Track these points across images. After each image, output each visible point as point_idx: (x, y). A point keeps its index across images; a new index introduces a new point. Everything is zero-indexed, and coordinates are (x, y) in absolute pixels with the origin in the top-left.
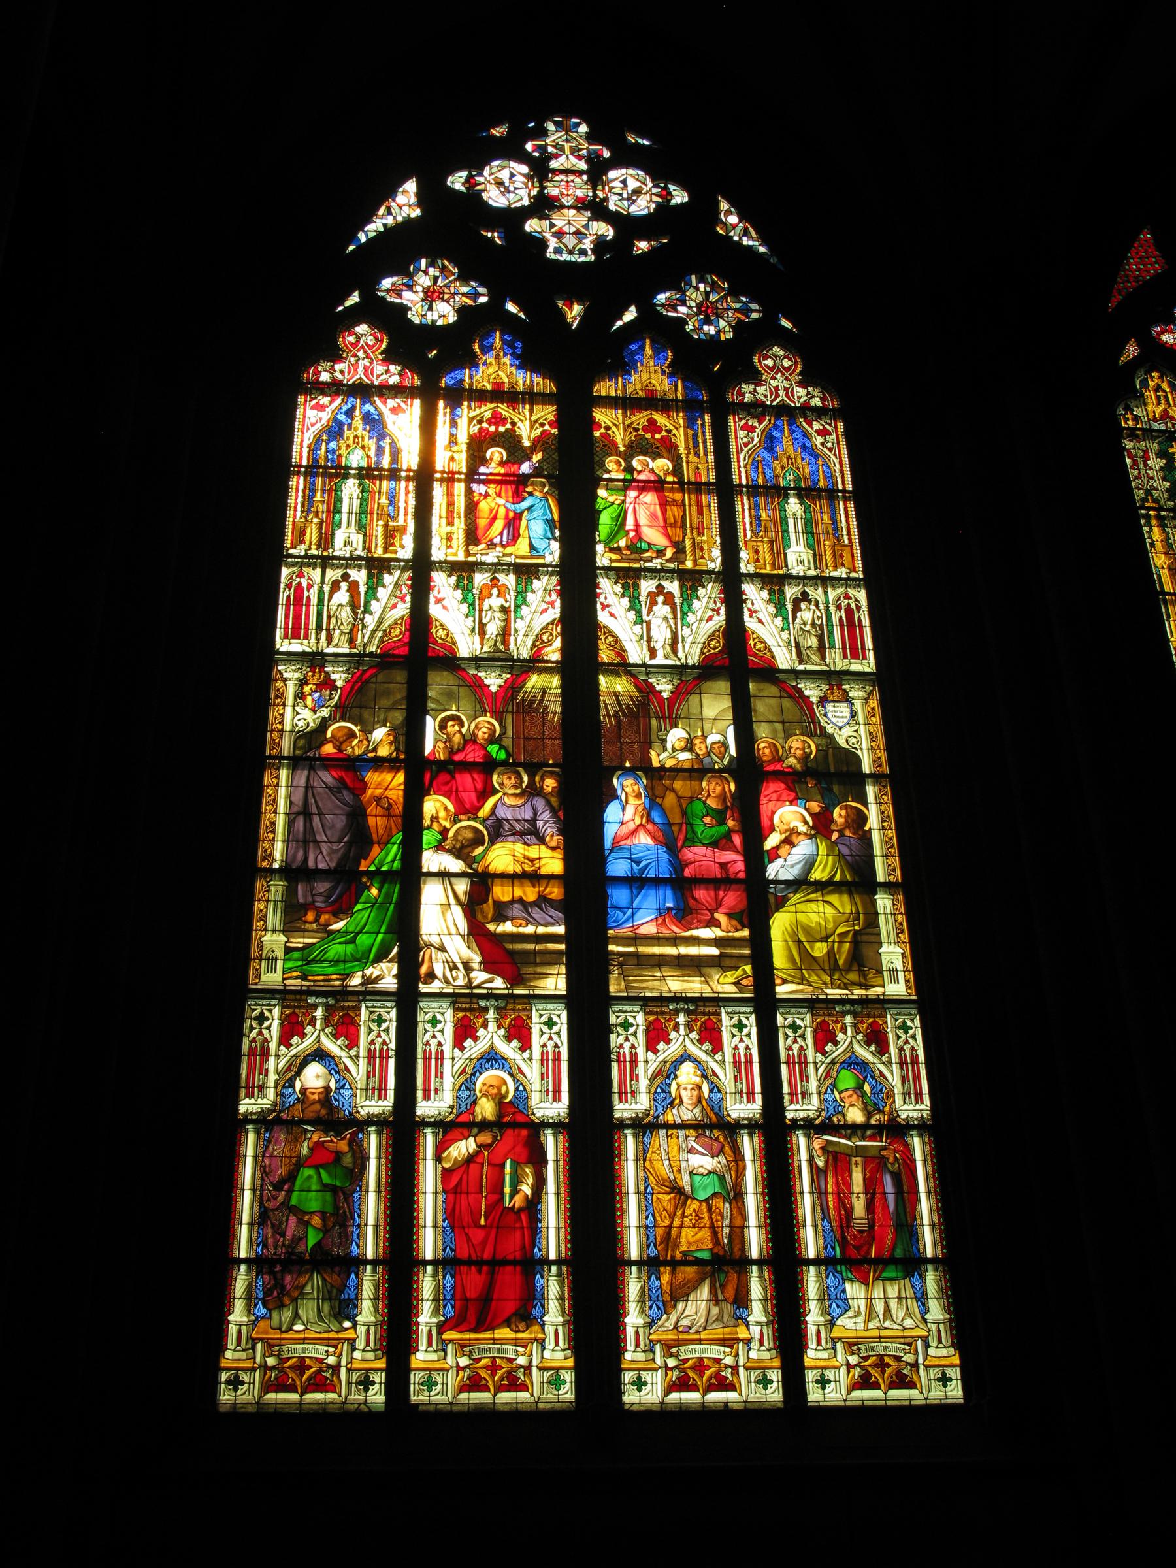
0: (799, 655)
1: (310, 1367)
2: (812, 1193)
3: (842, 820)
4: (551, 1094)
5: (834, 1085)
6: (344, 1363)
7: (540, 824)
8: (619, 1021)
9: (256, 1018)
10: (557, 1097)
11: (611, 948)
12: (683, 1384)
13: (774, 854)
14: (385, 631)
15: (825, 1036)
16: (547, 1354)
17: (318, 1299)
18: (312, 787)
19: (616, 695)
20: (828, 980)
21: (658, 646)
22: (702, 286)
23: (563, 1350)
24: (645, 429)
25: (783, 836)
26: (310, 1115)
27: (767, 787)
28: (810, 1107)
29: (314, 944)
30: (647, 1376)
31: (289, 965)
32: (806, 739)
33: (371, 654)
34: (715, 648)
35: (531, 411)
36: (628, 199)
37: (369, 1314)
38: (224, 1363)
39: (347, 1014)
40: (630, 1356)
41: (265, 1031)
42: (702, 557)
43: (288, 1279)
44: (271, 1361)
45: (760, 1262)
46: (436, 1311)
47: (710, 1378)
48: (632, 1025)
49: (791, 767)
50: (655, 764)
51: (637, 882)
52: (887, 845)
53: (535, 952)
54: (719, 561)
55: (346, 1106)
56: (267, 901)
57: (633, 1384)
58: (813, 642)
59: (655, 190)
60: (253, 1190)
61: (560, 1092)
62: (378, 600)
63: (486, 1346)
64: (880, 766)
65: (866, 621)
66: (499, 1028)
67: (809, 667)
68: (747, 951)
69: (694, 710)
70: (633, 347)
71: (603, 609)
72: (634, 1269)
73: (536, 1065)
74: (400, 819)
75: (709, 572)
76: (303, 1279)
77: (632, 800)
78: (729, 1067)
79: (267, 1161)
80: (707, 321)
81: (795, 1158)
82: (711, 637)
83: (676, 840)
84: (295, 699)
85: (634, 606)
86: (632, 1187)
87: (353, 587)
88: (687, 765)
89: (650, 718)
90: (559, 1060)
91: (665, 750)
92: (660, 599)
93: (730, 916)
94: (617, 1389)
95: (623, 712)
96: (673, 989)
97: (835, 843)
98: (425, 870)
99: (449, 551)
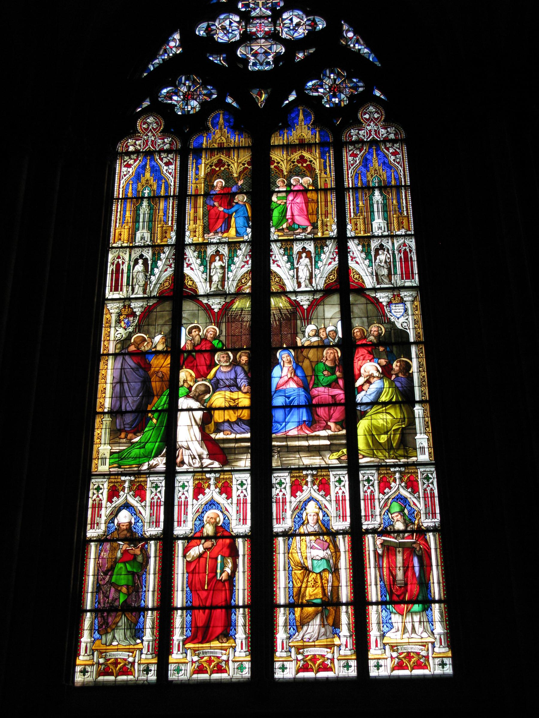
0: (377, 279)
1: (120, 663)
2: (375, 568)
3: (398, 368)
4: (242, 521)
5: (388, 510)
6: (137, 661)
7: (239, 380)
8: (277, 481)
9: (95, 489)
10: (245, 523)
11: (274, 443)
12: (305, 668)
13: (361, 389)
14: (161, 284)
15: (384, 484)
16: (237, 654)
17: (124, 629)
19: (280, 309)
20: (387, 454)
21: (302, 281)
22: (332, 75)
23: (245, 652)
24: (298, 162)
25: (366, 379)
26: (122, 536)
27: (358, 353)
28: (375, 522)
30: (287, 664)
31: (112, 461)
32: (380, 325)
33: (154, 297)
34: (332, 279)
35: (238, 157)
36: (293, 30)
37: (149, 636)
38: (78, 662)
39: (141, 485)
40: (279, 653)
41: (100, 495)
42: (327, 230)
43: (110, 619)
44: (101, 661)
45: (347, 604)
46: (182, 634)
47: (319, 665)
48: (284, 483)
49: (371, 341)
50: (299, 344)
51: (288, 407)
52: (421, 381)
54: (336, 231)
55: (140, 531)
56: (102, 429)
57: (280, 668)
58: (385, 272)
59: (308, 23)
60: (94, 575)
61: (246, 519)
62: (157, 268)
63: (207, 651)
64: (419, 337)
65: (415, 258)
66: (216, 488)
67: (383, 286)
68: (344, 442)
69: (321, 315)
70: (293, 115)
71: (274, 263)
72: (282, 609)
73: (235, 506)
74: (167, 383)
75: (330, 238)
76: (117, 619)
77: (286, 365)
78: (333, 503)
79: (100, 561)
80: (335, 96)
81: (367, 549)
82: (331, 274)
83: (309, 385)
85: (290, 260)
86: (282, 568)
87: (145, 261)
88: (316, 344)
89: (297, 320)
90: (246, 503)
91: (304, 336)
92: (304, 255)
93: (336, 423)
94: (272, 671)
95: (283, 318)
96: (305, 463)
97: (394, 381)
98: (180, 408)
99: (194, 238)
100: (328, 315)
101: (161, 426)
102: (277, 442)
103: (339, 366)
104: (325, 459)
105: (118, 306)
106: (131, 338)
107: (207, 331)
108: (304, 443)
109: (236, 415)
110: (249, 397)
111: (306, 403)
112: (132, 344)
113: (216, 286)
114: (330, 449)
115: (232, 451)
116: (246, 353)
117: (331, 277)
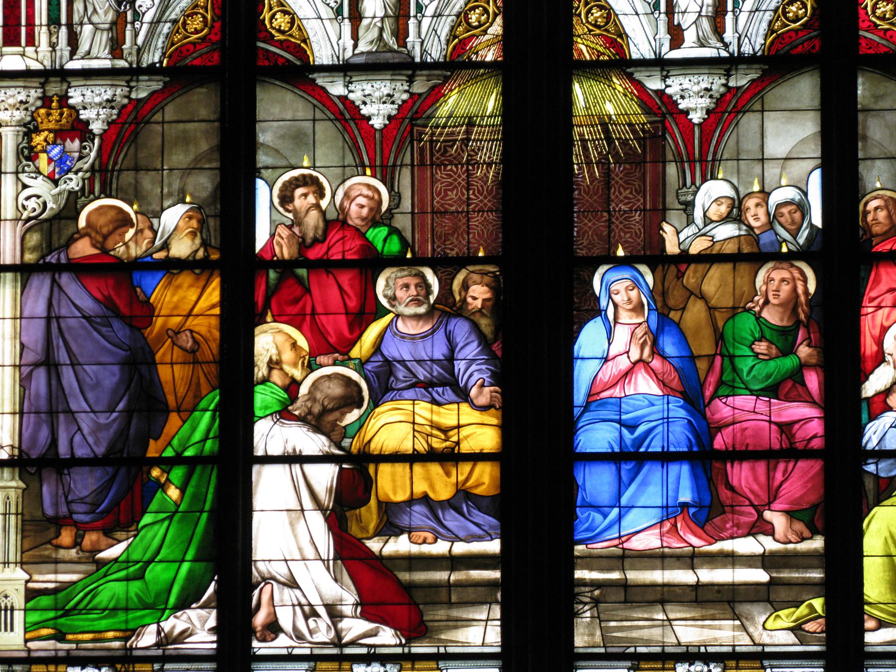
7: (460, 366)
11: (579, 574)
13: (880, 404)
14: (175, 22)
18: (58, 318)
19: (605, 123)
21: (686, 21)
27: (877, 282)
29: (74, 583)
31: (34, 617)
33: (152, 70)
50: (672, 248)
51: (630, 458)
53: (448, 585)
68: (816, 575)
69: (750, 145)
74: (213, 369)
77: (625, 317)
83: (702, 386)
84: (18, 159)
89: (664, 162)
91: (690, 221)
93: (791, 514)
95: (618, 161)
96: (683, 640)
98: (259, 452)
100: (776, 146)
101: (195, 509)
102: (591, 569)
103: (807, 327)
104: (751, 630)
105: (22, 97)
106: (78, 214)
107: (346, 195)
108: (683, 576)
109: (453, 479)
110: (495, 421)
111: (690, 446)
112: (81, 234)
113: (374, 33)
114: (768, 596)
115: (441, 595)
116: (484, 274)
117: (794, 8)
